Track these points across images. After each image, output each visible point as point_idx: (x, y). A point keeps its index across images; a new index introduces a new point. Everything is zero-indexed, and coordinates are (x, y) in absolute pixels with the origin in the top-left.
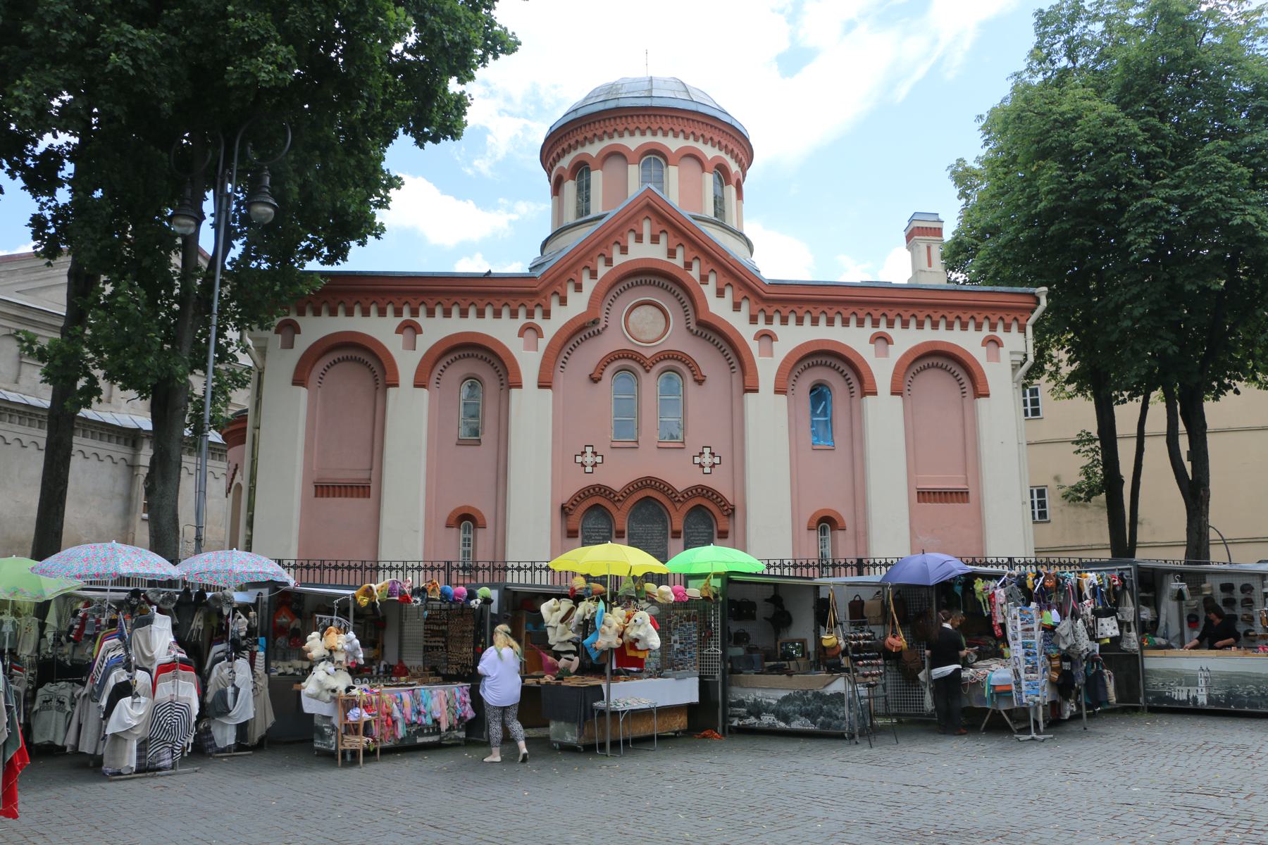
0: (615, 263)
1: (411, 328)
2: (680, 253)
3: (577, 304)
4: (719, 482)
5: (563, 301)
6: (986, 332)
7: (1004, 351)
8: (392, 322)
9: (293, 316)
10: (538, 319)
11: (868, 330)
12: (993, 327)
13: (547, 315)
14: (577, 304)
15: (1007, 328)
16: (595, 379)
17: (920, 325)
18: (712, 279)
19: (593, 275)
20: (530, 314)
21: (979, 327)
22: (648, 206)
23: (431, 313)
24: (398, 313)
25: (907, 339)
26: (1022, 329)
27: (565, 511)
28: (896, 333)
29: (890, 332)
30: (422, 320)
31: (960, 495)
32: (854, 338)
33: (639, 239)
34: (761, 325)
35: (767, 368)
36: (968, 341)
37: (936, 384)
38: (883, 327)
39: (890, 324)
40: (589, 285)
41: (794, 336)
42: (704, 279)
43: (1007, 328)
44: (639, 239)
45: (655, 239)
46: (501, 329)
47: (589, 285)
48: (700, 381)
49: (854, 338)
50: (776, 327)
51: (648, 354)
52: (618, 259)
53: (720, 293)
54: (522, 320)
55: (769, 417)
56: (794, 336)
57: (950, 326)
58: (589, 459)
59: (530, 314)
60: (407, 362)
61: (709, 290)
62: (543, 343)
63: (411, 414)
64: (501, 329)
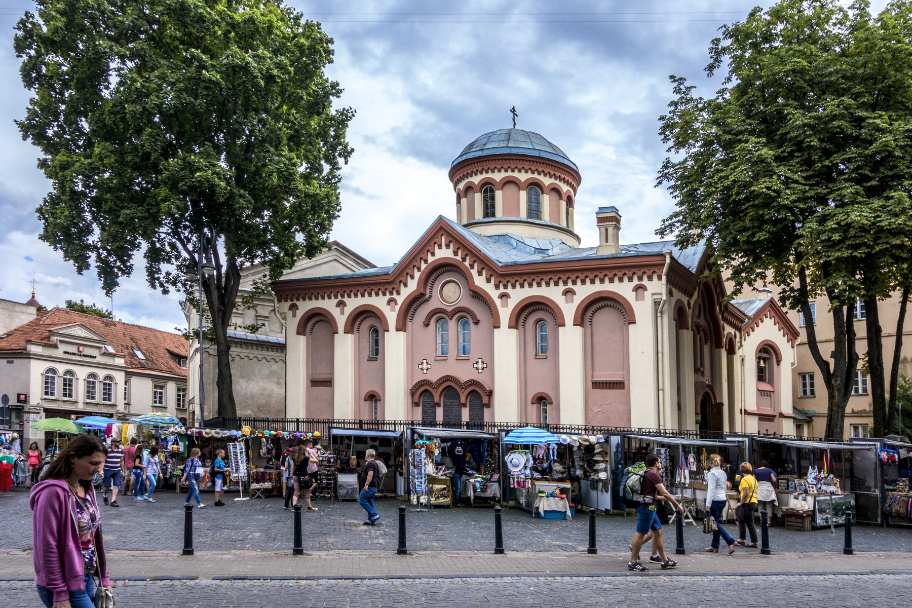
1: (341, 304)
5: (406, 285)
6: (636, 282)
8: (334, 301)
9: (295, 302)
10: (395, 296)
11: (562, 287)
13: (398, 293)
14: (412, 286)
16: (427, 325)
22: (441, 228)
24: (336, 297)
29: (574, 287)
30: (346, 300)
34: (502, 290)
35: (505, 314)
38: (570, 285)
40: (417, 275)
41: (519, 294)
42: (472, 266)
45: (448, 246)
46: (379, 302)
47: (417, 275)
48: (477, 322)
50: (510, 290)
53: (480, 273)
55: (506, 343)
56: (519, 294)
58: (425, 366)
60: (341, 321)
61: (474, 272)
63: (346, 347)
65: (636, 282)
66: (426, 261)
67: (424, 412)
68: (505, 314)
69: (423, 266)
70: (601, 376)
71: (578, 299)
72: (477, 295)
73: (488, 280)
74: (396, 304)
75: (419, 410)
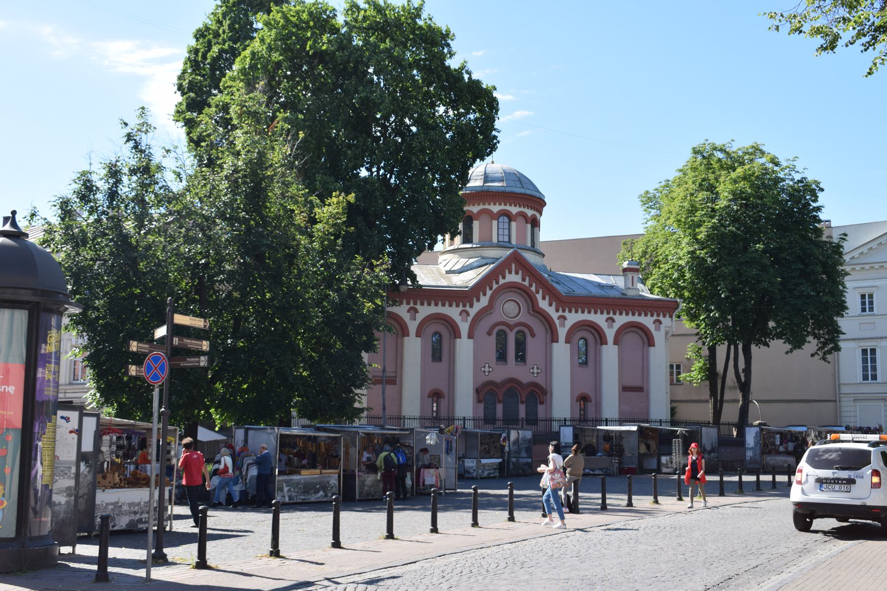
2: (527, 278)
3: (484, 301)
4: (541, 381)
5: (478, 300)
6: (655, 317)
7: (662, 326)
10: (468, 308)
11: (605, 316)
12: (658, 315)
13: (471, 306)
14: (484, 301)
15: (664, 316)
17: (627, 314)
18: (541, 291)
19: (491, 289)
20: (464, 306)
21: (652, 315)
23: (422, 304)
25: (621, 319)
26: (671, 317)
27: (477, 391)
28: (617, 317)
29: (614, 317)
31: (640, 389)
32: (599, 319)
33: (510, 272)
34: (560, 313)
35: (562, 333)
36: (647, 321)
37: (633, 339)
38: (611, 315)
39: (615, 314)
40: (489, 293)
41: (573, 318)
42: (537, 292)
43: (664, 316)
44: (510, 272)
45: (517, 273)
46: (453, 312)
47: (489, 293)
48: (533, 335)
49: (599, 319)
50: (567, 314)
52: (502, 281)
53: (544, 298)
54: (461, 308)
56: (573, 318)
57: (640, 315)
58: (487, 369)
59: (464, 306)
61: (539, 296)
62: (470, 319)
64: (453, 312)
65: (655, 317)
66: (497, 283)
67: (485, 408)
69: (495, 286)
70: (629, 383)
71: (617, 326)
73: (550, 305)
75: (482, 405)
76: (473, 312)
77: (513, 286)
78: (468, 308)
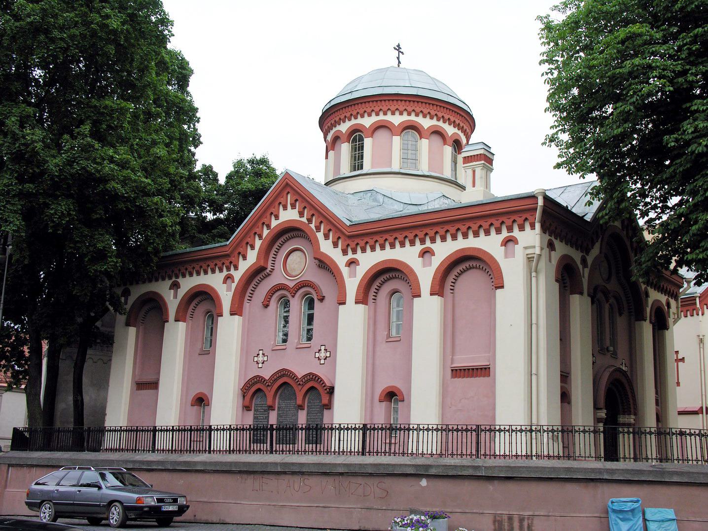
0: (272, 227)
3: (252, 256)
5: (245, 258)
13: (236, 268)
14: (252, 256)
19: (260, 237)
34: (350, 255)
40: (258, 243)
41: (369, 260)
42: (318, 229)
45: (293, 206)
47: (258, 243)
50: (359, 256)
51: (291, 285)
53: (326, 237)
55: (352, 321)
61: (320, 235)
66: (268, 226)
68: (352, 285)
69: (266, 232)
72: (324, 264)
73: (335, 245)
74: (233, 282)
76: (238, 275)
77: (290, 231)
78: (232, 272)
